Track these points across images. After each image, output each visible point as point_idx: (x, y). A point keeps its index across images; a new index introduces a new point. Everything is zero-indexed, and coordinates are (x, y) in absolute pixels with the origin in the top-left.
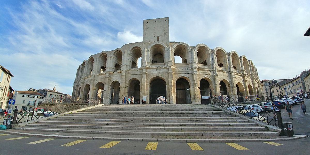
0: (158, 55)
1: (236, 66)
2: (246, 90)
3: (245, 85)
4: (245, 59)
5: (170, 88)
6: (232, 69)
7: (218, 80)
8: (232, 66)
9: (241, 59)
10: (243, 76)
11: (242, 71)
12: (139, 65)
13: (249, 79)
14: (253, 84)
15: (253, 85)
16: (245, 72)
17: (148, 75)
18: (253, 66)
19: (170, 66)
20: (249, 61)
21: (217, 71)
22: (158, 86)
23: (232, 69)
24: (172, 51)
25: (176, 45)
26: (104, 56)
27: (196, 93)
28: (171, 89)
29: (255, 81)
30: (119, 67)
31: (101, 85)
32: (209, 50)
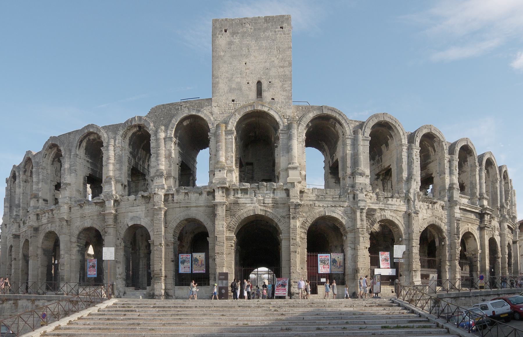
0: (258, 141)
1: (467, 183)
2: (483, 252)
3: (482, 238)
4: (490, 163)
5: (292, 250)
6: (457, 194)
7: (419, 225)
8: (457, 186)
9: (481, 165)
10: (481, 216)
11: (481, 198)
12: (202, 179)
13: (495, 223)
14: (500, 235)
15: (501, 237)
16: (485, 203)
17: (230, 210)
18: (508, 183)
19: (293, 184)
20: (500, 168)
21: (417, 200)
22: (259, 243)
23: (457, 194)
24: (299, 135)
25: (311, 115)
26: (93, 145)
27: (360, 265)
28: (296, 252)
29: (506, 227)
30: (141, 178)
31: (95, 237)
32: (401, 134)
